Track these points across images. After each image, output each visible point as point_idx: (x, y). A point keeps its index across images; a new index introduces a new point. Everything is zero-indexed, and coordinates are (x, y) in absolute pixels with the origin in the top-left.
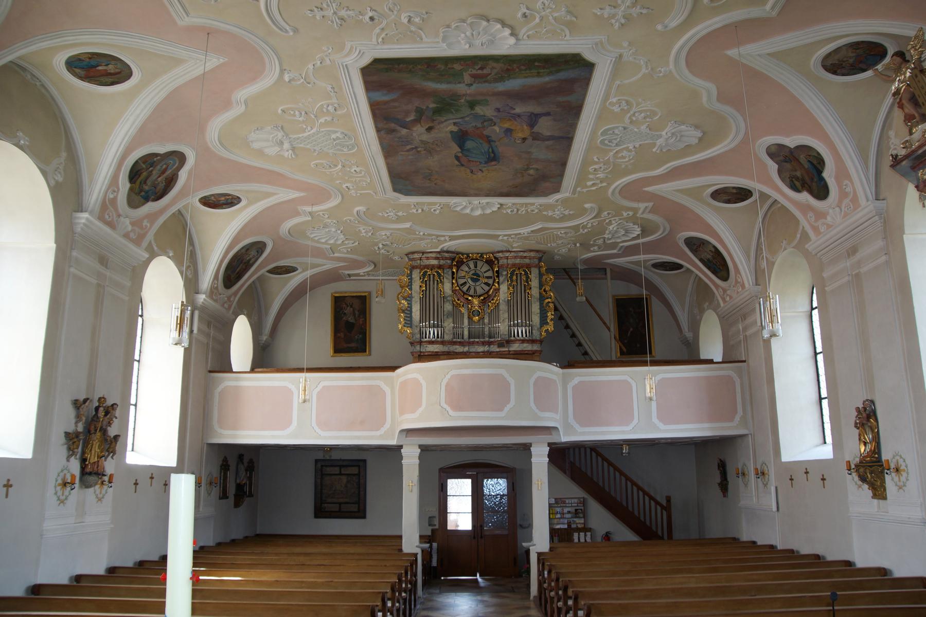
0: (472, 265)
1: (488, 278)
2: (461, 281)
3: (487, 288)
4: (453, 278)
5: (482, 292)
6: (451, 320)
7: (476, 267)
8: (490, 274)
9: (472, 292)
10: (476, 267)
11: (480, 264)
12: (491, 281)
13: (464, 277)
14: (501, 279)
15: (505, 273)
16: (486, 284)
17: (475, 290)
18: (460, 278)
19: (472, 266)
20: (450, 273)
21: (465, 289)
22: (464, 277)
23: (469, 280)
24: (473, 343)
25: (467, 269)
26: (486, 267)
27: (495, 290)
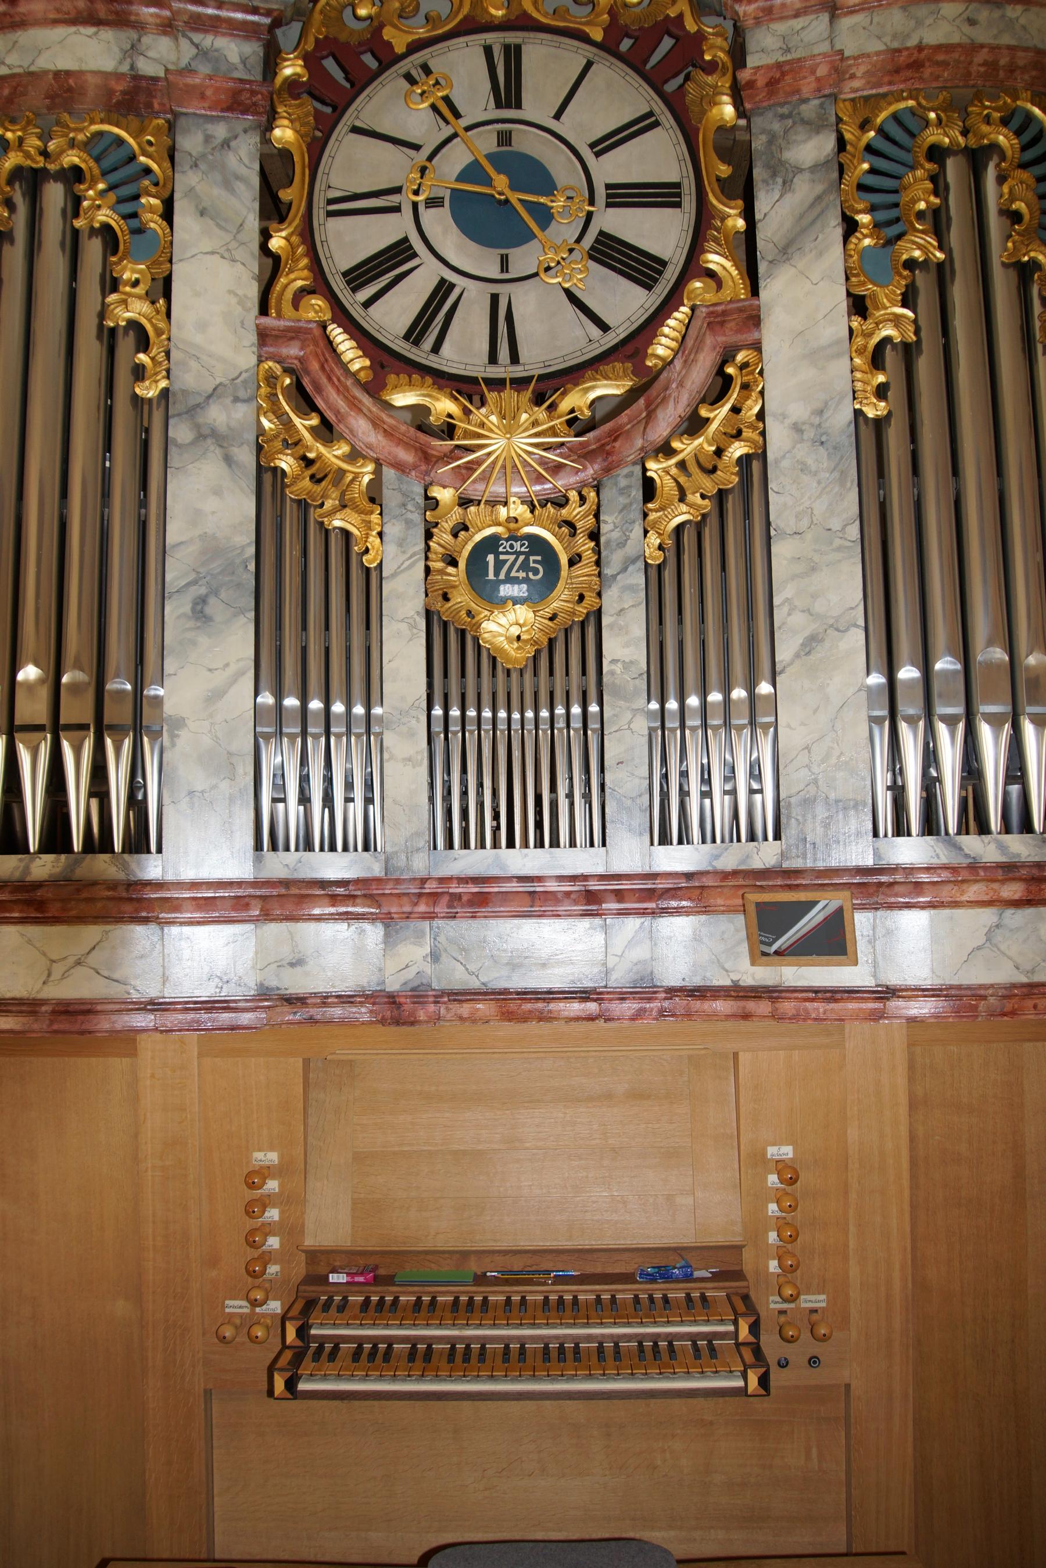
0: (464, 69)
1: (622, 196)
2: (350, 241)
3: (624, 303)
4: (272, 209)
5: (576, 340)
6: (237, 643)
7: (508, 92)
8: (658, 157)
9: (464, 348)
10: (508, 92)
11: (547, 66)
12: (660, 233)
13: (380, 201)
14: (776, 210)
15: (812, 149)
16: (611, 253)
17: (502, 323)
18: (349, 205)
19: (474, 95)
20: (244, 159)
21: (393, 314)
22: (380, 201)
23: (440, 225)
24: (480, 898)
25: (416, 120)
26: (614, 96)
27: (717, 319)
